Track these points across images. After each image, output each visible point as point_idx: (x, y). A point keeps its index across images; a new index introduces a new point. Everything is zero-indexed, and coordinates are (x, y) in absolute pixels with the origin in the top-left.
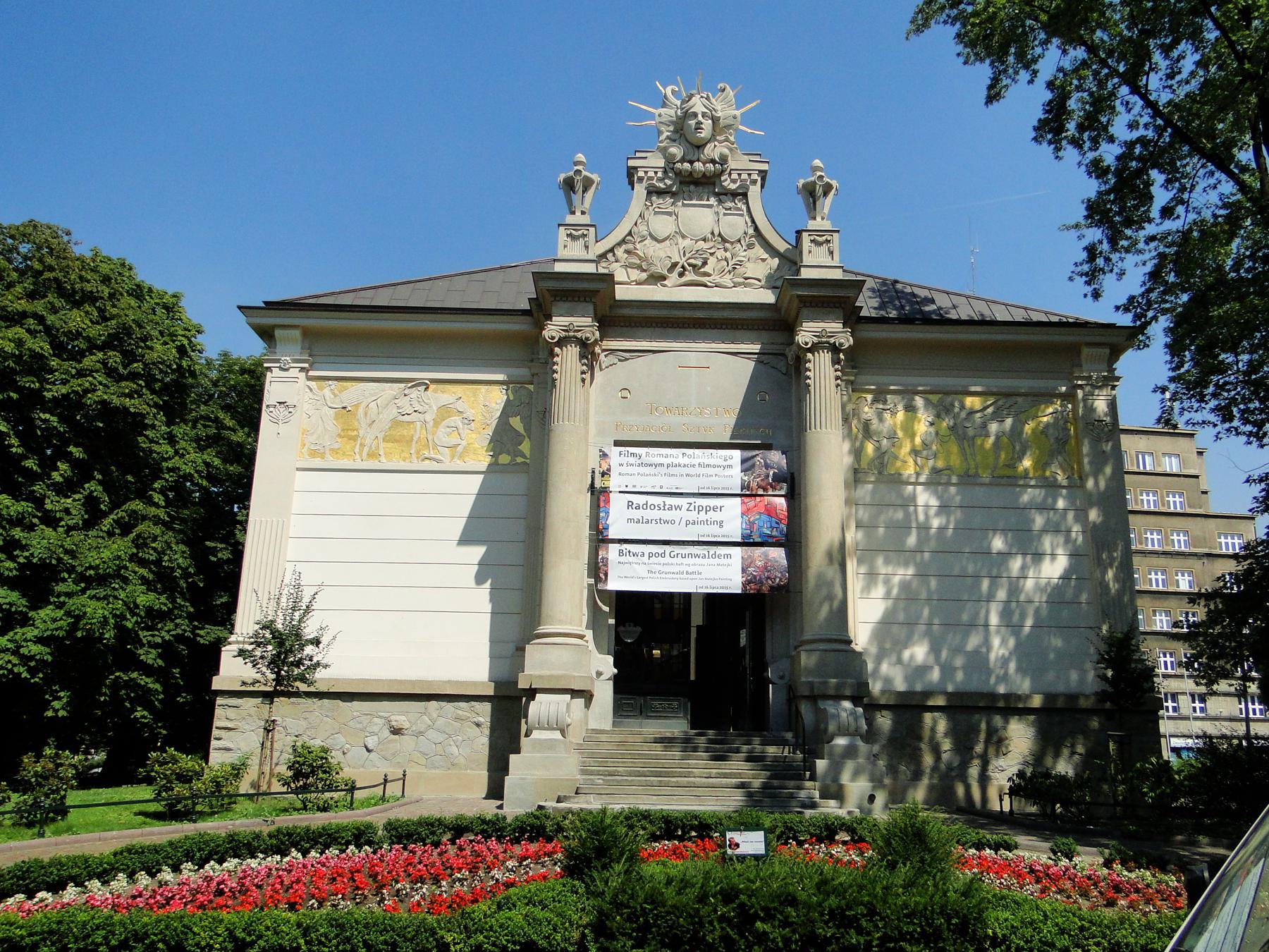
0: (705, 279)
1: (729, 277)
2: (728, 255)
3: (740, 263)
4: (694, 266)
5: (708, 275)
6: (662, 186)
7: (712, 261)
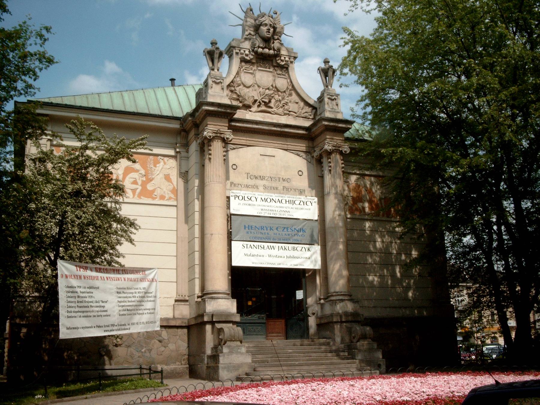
0: (270, 110)
1: (281, 110)
2: (280, 98)
3: (286, 104)
4: (265, 102)
5: (272, 108)
6: (248, 58)
7: (273, 101)
